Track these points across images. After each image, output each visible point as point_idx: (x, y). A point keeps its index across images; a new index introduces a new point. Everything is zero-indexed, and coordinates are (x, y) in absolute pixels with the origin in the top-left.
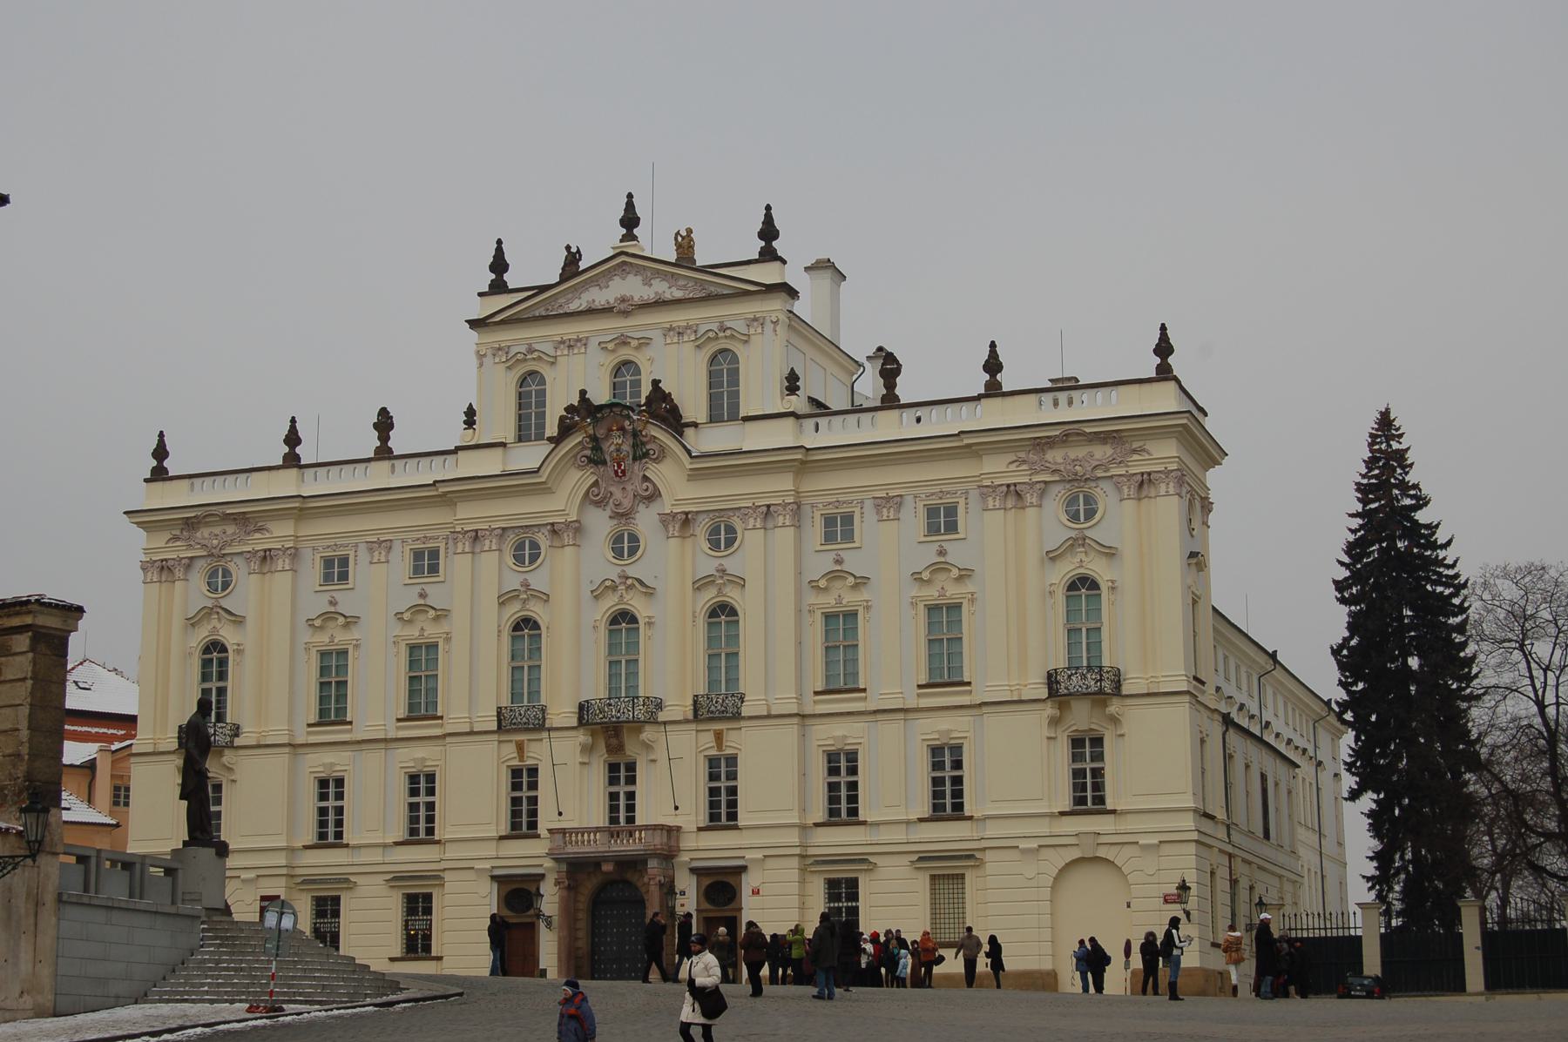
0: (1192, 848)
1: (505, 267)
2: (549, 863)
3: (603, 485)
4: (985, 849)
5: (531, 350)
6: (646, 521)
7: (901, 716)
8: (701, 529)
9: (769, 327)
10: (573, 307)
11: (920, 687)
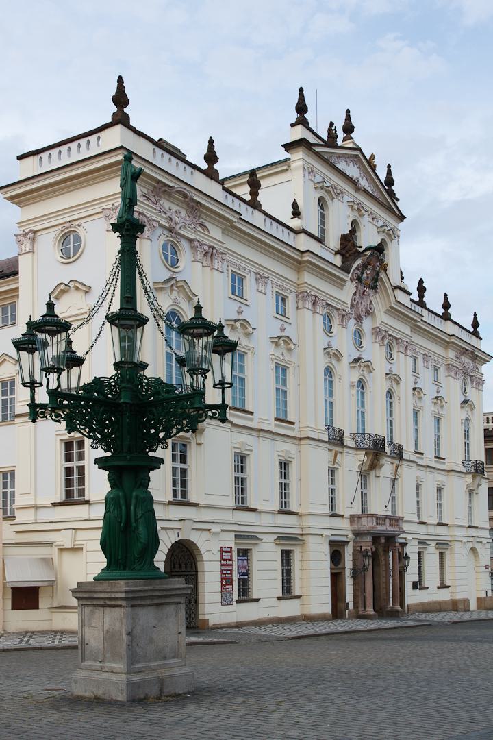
0: (488, 546)
2: (351, 536)
3: (358, 294)
4: (450, 541)
6: (367, 324)
7: (432, 470)
8: (386, 341)
11: (435, 457)
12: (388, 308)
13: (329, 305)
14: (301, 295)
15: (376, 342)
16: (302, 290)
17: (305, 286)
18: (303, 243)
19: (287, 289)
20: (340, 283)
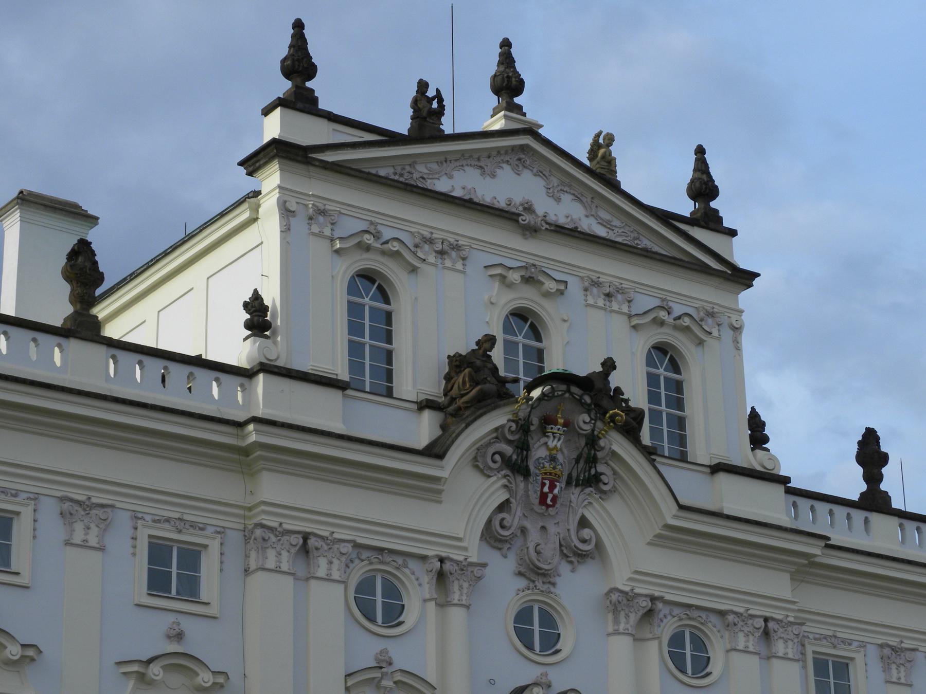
1: (310, 71)
3: (518, 510)
5: (377, 236)
6: (577, 593)
9: (727, 334)
10: (442, 185)
12: (658, 531)
13: (381, 550)
14: (258, 535)
15: (617, 633)
16: (250, 523)
17: (264, 512)
18: (261, 396)
19: (193, 525)
20: (429, 490)
